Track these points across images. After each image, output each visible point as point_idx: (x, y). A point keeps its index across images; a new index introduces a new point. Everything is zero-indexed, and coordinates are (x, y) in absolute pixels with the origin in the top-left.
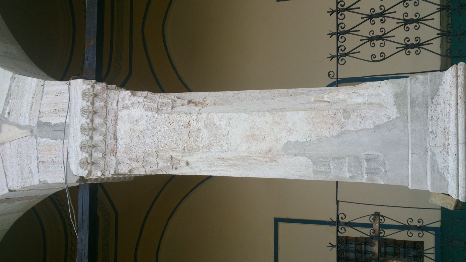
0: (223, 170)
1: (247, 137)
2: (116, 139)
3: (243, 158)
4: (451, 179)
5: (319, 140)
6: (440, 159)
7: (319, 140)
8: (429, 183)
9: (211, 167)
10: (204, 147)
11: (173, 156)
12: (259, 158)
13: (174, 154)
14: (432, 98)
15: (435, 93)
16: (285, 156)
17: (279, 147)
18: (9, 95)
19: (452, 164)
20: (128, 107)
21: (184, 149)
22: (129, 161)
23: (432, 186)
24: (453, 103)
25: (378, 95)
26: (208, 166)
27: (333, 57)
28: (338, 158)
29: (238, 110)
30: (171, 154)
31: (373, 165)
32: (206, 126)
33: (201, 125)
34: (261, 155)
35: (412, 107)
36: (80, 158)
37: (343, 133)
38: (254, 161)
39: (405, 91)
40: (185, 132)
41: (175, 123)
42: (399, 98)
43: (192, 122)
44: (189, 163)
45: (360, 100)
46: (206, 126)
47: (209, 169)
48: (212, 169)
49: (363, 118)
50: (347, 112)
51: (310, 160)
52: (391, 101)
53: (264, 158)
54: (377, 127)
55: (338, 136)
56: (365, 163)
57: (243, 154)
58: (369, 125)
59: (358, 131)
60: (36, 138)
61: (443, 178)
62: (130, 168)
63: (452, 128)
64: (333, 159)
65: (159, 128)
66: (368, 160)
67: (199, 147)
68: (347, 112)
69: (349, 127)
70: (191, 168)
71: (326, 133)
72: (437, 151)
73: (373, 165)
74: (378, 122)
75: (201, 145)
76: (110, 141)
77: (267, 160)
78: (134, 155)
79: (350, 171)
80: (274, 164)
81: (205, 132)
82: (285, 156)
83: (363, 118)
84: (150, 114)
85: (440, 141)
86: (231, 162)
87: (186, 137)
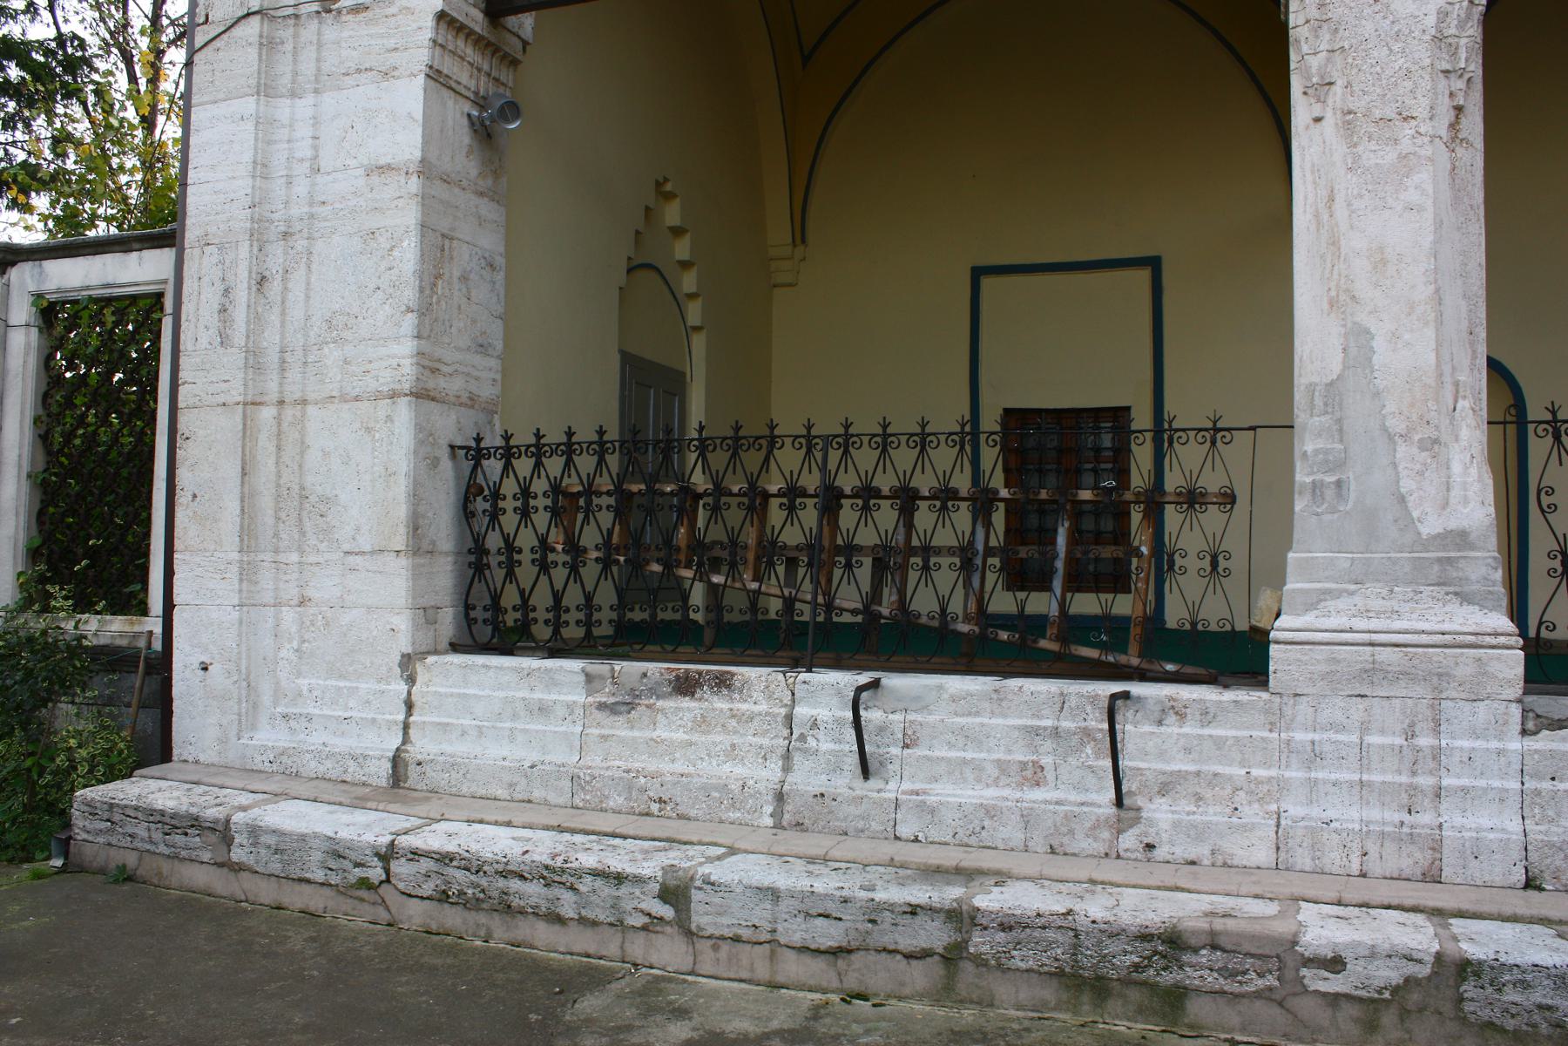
1: (1381, 249)
3: (1334, 243)
4: (1308, 619)
5: (1377, 394)
6: (1342, 603)
7: (1377, 394)
8: (1299, 585)
10: (1357, 158)
11: (1333, 88)
12: (1335, 276)
13: (1338, 89)
14: (1456, 594)
15: (1465, 598)
17: (1363, 318)
23: (1294, 590)
24: (1446, 627)
25: (1466, 501)
27: (1554, 413)
28: (1341, 430)
29: (1439, 224)
30: (1340, 83)
31: (1330, 493)
32: (1403, 157)
33: (1406, 145)
35: (1439, 560)
37: (1391, 438)
39: (1473, 547)
40: (1390, 112)
41: (1408, 84)
42: (1460, 538)
43: (1413, 123)
44: (1318, 125)
45: (1456, 468)
46: (1403, 157)
47: (1308, 166)
48: (1308, 174)
49: (1421, 473)
50: (1432, 445)
52: (1453, 525)
53: (1338, 286)
54: (1402, 500)
55: (1384, 429)
56: (1333, 479)
57: (1343, 242)
58: (1407, 485)
59: (1395, 465)
61: (1310, 607)
63: (1398, 625)
64: (1339, 421)
65: (1396, 47)
66: (1339, 484)
67: (1355, 145)
68: (1432, 445)
69: (1402, 449)
70: (1307, 128)
71: (1391, 407)
72: (1357, 599)
73: (1330, 493)
74: (1411, 501)
75: (1360, 149)
77: (1333, 293)
79: (1317, 452)
80: (1326, 306)
81: (1389, 156)
83: (1421, 473)
84: (1431, 20)
85: (1377, 604)
86: (1326, 217)
87: (1377, 114)
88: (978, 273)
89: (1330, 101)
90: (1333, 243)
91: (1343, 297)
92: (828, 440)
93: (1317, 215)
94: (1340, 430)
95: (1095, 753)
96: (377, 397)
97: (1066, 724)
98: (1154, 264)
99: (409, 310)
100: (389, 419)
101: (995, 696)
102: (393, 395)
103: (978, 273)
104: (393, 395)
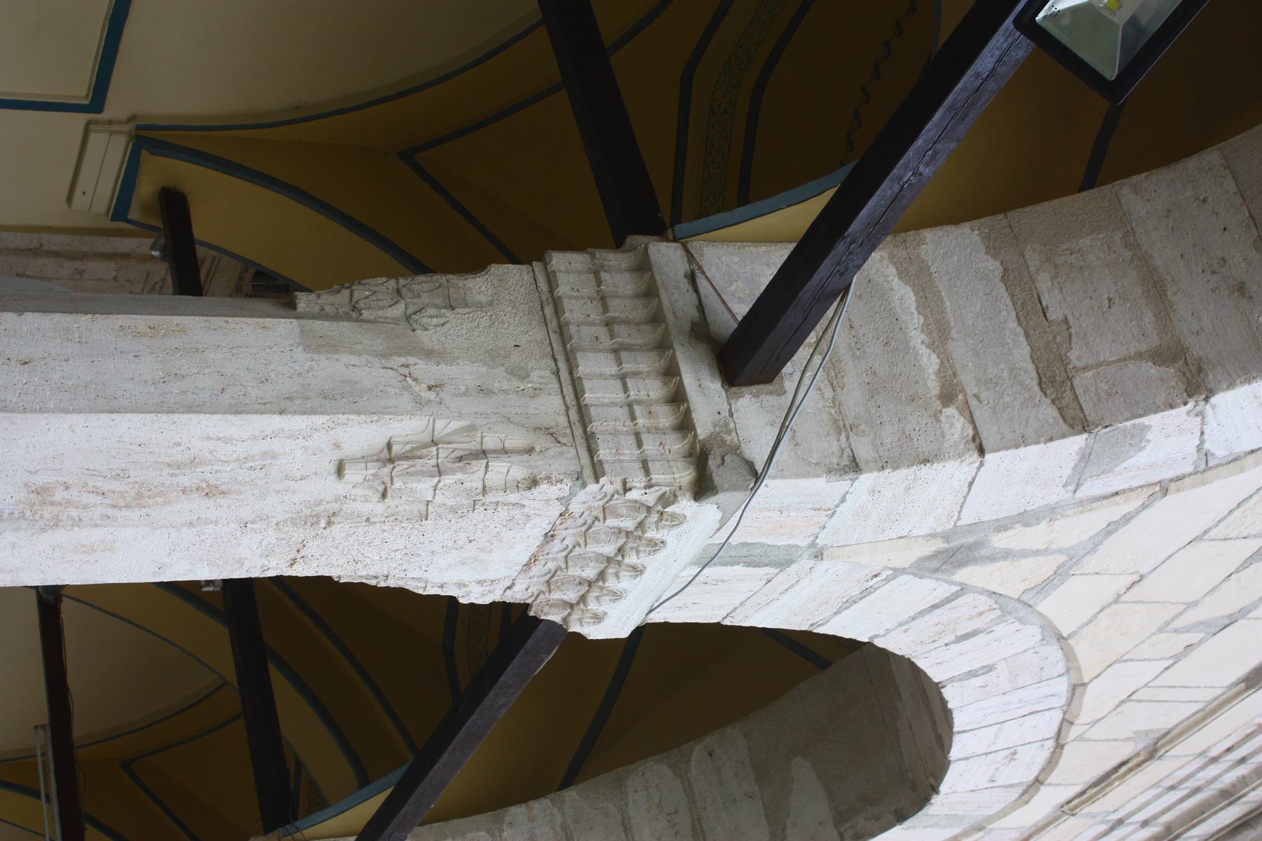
0: (228, 441)
2: (549, 536)
3: (141, 497)
9: (265, 455)
18: (849, 603)
20: (480, 583)
21: (329, 524)
22: (526, 503)
26: (274, 457)
30: (380, 508)
34: (74, 513)
36: (676, 531)
38: (105, 486)
44: (332, 468)
53: (69, 503)
57: (136, 513)
60: (813, 545)
62: (528, 494)
70: (337, 446)
75: (271, 532)
77: (59, 495)
78: (503, 513)
80: (40, 480)
86: (185, 481)
89: (359, 492)
90: (140, 495)
91: (48, 512)
93: (194, 462)
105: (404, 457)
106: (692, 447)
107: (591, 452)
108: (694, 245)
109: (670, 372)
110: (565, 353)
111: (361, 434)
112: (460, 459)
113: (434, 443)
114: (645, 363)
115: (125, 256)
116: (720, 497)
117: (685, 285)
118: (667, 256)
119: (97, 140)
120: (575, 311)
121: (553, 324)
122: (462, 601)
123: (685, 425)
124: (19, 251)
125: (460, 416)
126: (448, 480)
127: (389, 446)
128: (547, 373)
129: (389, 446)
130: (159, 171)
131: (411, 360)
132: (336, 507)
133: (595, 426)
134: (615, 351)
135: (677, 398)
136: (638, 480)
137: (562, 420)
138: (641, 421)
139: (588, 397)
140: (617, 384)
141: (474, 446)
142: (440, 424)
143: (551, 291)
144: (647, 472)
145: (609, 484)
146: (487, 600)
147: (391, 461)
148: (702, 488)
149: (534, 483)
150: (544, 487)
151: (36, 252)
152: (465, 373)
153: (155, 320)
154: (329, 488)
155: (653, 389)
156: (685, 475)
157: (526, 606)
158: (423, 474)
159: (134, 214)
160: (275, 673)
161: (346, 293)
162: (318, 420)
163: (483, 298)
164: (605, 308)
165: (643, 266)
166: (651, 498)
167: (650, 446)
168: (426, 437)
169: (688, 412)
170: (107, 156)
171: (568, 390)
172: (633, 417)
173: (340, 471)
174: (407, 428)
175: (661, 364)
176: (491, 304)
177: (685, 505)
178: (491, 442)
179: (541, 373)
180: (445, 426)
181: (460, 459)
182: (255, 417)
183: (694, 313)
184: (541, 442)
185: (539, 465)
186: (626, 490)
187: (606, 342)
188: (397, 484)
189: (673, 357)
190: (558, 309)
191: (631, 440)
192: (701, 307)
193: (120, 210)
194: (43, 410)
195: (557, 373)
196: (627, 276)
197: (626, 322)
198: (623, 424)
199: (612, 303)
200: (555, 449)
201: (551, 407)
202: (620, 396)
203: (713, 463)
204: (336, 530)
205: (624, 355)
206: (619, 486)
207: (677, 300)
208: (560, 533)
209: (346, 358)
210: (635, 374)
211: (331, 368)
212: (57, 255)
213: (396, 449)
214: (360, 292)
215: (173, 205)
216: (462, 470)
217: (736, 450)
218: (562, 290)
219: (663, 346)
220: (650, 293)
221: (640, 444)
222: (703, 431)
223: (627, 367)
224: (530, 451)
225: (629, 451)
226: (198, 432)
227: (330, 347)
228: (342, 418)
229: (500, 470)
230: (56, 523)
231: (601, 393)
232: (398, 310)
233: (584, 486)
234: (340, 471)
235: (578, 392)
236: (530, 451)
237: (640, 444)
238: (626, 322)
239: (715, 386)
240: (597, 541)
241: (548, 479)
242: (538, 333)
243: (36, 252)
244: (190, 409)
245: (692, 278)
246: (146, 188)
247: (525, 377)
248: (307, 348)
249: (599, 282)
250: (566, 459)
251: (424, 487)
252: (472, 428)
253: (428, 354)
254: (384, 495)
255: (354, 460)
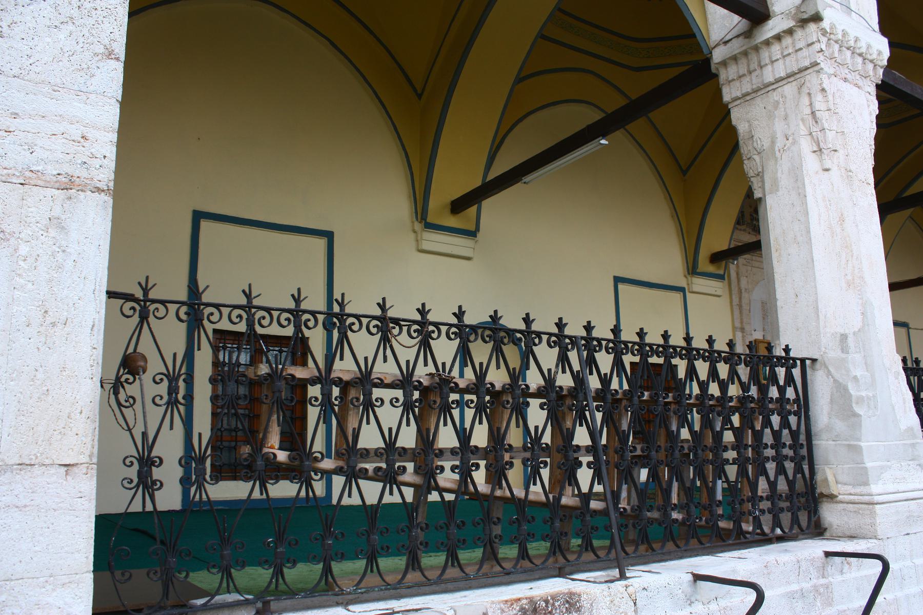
2: (845, 80)
14: (919, 465)
16: (860, 301)
19: (891, 487)
20: (869, 106)
30: (841, 153)
36: (837, 26)
44: (826, 173)
51: (857, 330)
63: (911, 486)
66: (874, 396)
74: (896, 408)
76: (844, 72)
77: (849, 277)
78: (838, 101)
82: (860, 301)
88: (198, 216)
89: (835, 161)
90: (846, 247)
92: (574, 340)
94: (868, 366)
95: (822, 604)
96: (28, 180)
97: (806, 585)
98: (329, 236)
99: (110, 54)
100: (56, 223)
101: (765, 572)
102: (68, 185)
103: (198, 216)
104: (68, 185)
105: (818, 145)
106: (799, 26)
107: (807, 68)
108: (712, 44)
109: (767, 43)
110: (765, 88)
111: (811, 163)
112: (816, 122)
113: (811, 134)
114: (765, 54)
115: (738, 274)
116: (820, 10)
117: (729, 45)
118: (718, 55)
119: (695, 288)
120: (747, 87)
121: (754, 95)
122: (877, 112)
123: (790, 32)
124: (741, 312)
125: (798, 125)
126: (826, 126)
127: (815, 152)
128: (775, 94)
129: (815, 152)
130: (704, 265)
131: (777, 149)
132: (843, 170)
133: (795, 69)
134: (761, 67)
135: (778, 38)
136: (817, 47)
137: (794, 83)
138: (790, 51)
139: (783, 74)
140: (775, 64)
141: (810, 117)
142: (802, 133)
143: (740, 98)
144: (813, 43)
145: (820, 58)
146: (876, 102)
147: (820, 150)
148: (817, 18)
149: (823, 90)
150: (824, 86)
151: (740, 306)
152: (779, 127)
153: (773, 250)
154: (835, 173)
155: (776, 49)
156: (812, 27)
157: (877, 86)
158: (825, 136)
159: (721, 272)
160: (908, 193)
161: (752, 179)
162: (807, 182)
163: (747, 125)
164: (744, 75)
165: (724, 63)
166: (824, 40)
167: (801, 44)
168: (809, 138)
169: (784, 32)
170: (700, 284)
171: (781, 84)
172: (789, 54)
173: (827, 170)
174: (806, 146)
175: (764, 48)
176: (749, 122)
177: (825, 24)
178: (807, 111)
179: (775, 96)
180: (803, 130)
181: (816, 122)
182: (809, 206)
183: (741, 38)
184: (805, 90)
185: (815, 89)
186: (822, 51)
187: (758, 72)
188: (830, 146)
189: (761, 43)
190: (748, 94)
191: (799, 53)
192: (738, 36)
193: (721, 277)
194: (816, 287)
195: (774, 89)
196: (729, 69)
197: (748, 66)
198: (793, 58)
199: (741, 73)
200: (807, 84)
201: (789, 89)
202: (781, 62)
203: (805, 16)
204: (853, 168)
205: (762, 64)
206: (820, 54)
207: (736, 46)
208: (844, 76)
209: (779, 175)
210: (770, 57)
211: (784, 180)
212: (740, 298)
213: (815, 149)
214: (751, 174)
215: (716, 258)
216: (821, 120)
217: (798, 8)
218: (739, 94)
219: (756, 49)
220: (735, 58)
221: (801, 49)
222: (792, 24)
223: (767, 61)
224: (809, 94)
225: (805, 52)
226: (817, 228)
227: (775, 182)
228: (805, 172)
229: (819, 104)
230: (862, 278)
231: (781, 70)
232: (756, 157)
233: (822, 69)
234: (827, 170)
235: (782, 79)
236: (809, 94)
237: (801, 49)
238: (748, 66)
239: (771, 23)
240: (845, 59)
241: (820, 84)
242: (758, 101)
243: (740, 306)
244: (809, 232)
245: (726, 43)
246: (711, 269)
247: (778, 102)
248: (777, 190)
249: (733, 80)
250: (811, 79)
251: (830, 135)
252: (803, 120)
253: (773, 143)
254: (835, 151)
255: (822, 165)
